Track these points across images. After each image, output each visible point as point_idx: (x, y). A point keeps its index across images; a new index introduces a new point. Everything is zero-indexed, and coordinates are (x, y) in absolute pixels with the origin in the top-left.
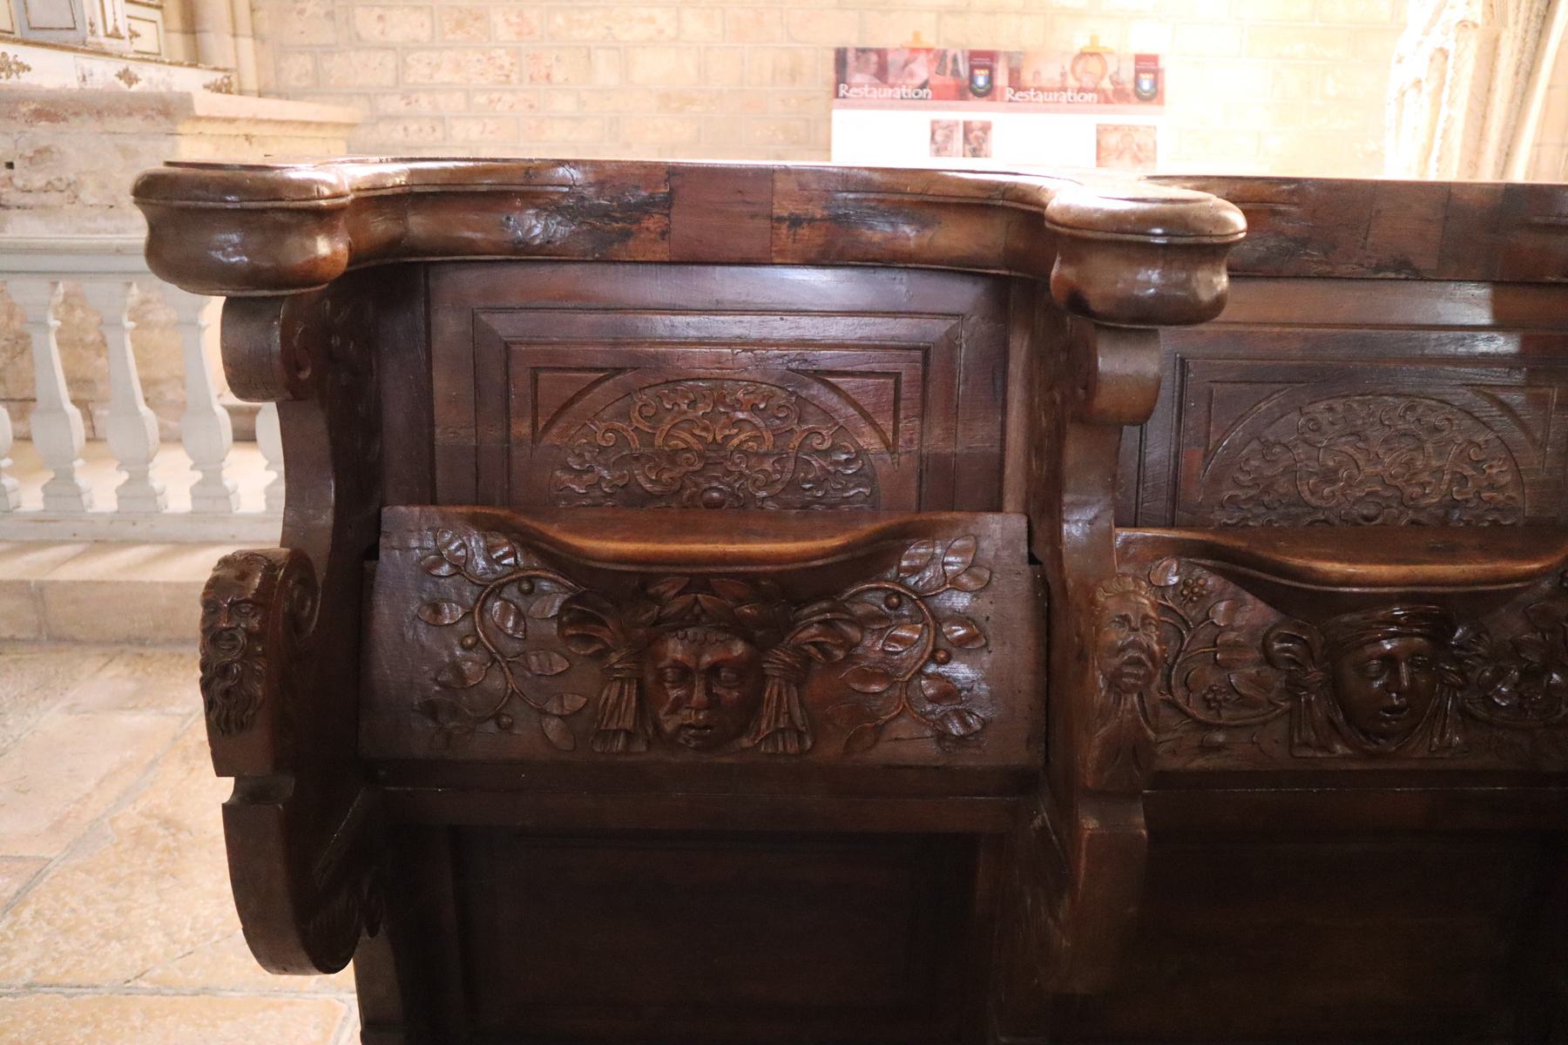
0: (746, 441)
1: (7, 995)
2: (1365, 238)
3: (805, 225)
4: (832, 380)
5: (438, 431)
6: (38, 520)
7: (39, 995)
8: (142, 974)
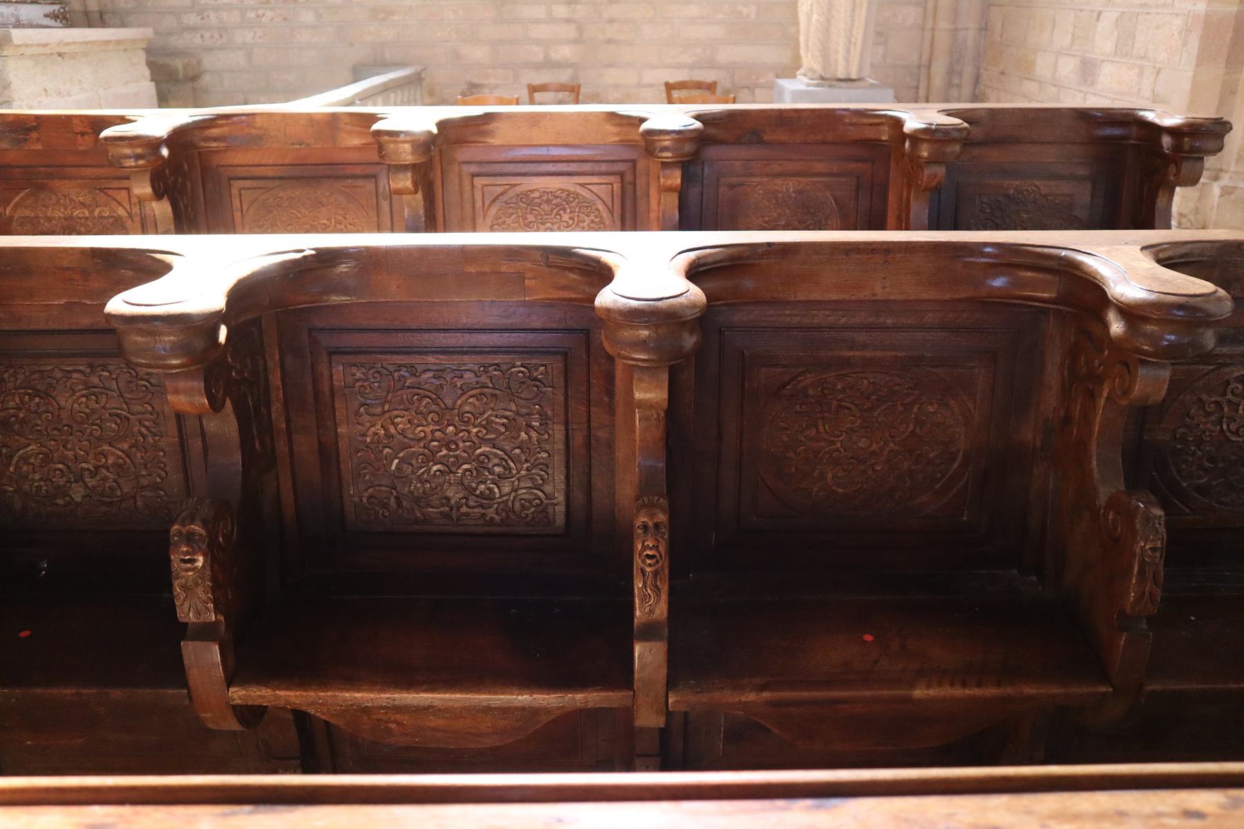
0: (79, 213)
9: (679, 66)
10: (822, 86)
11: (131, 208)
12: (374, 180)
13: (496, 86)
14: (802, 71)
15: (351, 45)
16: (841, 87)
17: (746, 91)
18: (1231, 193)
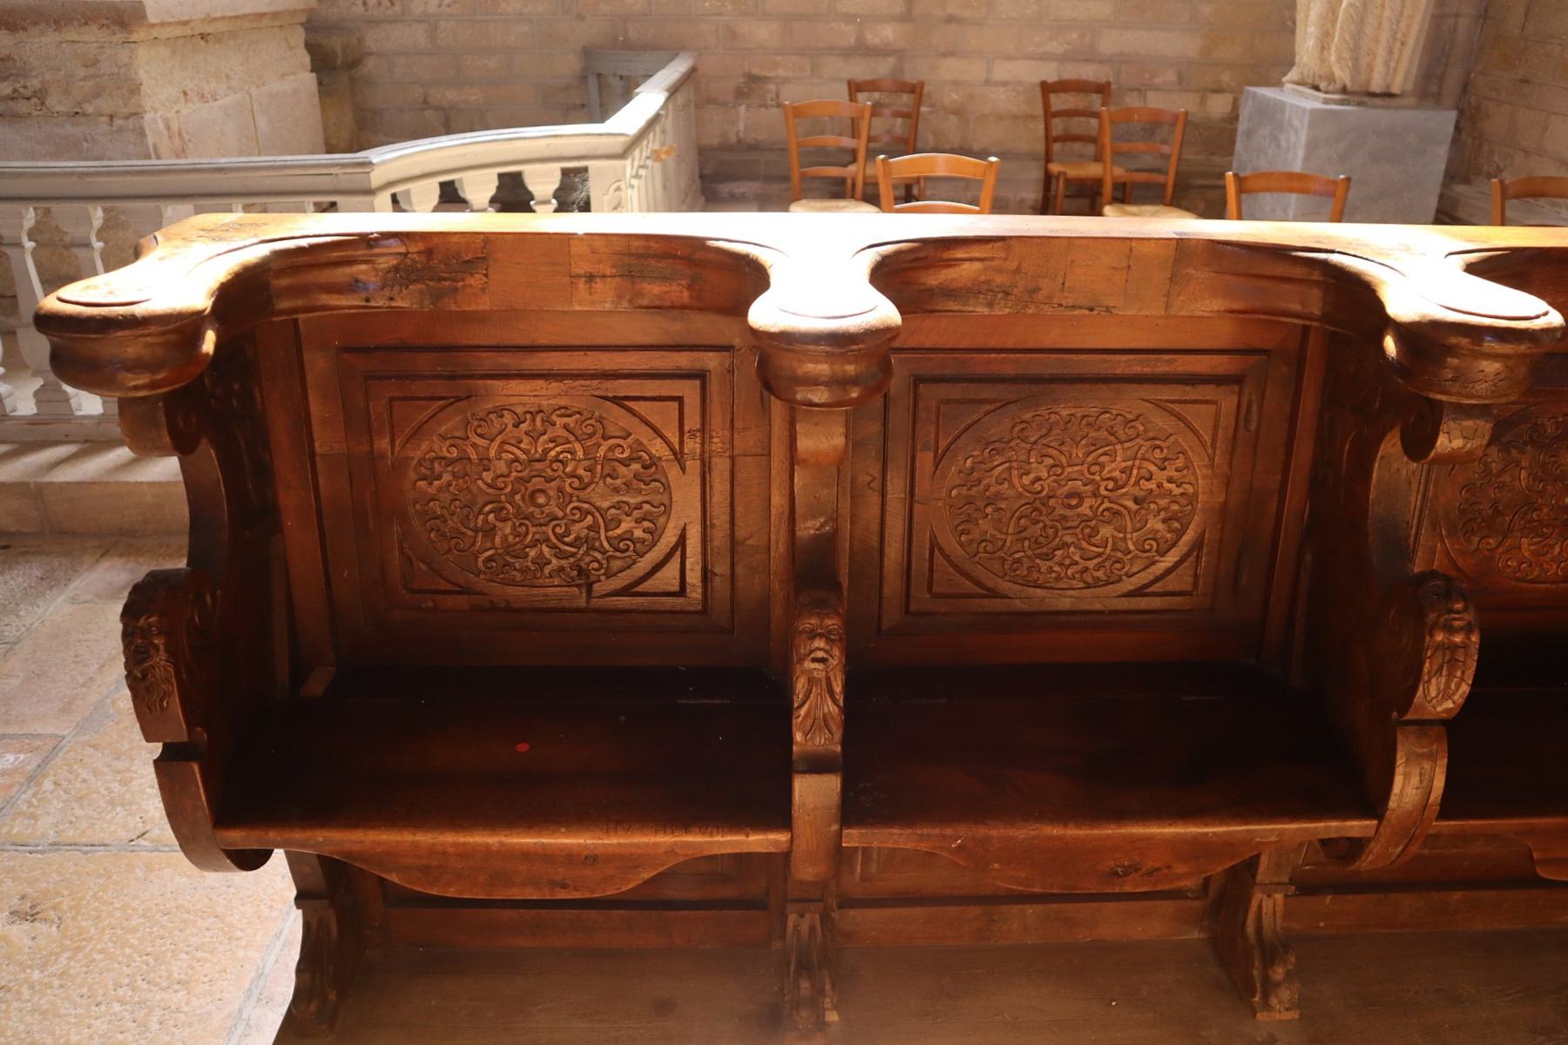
0: (562, 452)
1: (35, 852)
2: (1063, 284)
3: (598, 280)
4: (627, 403)
5: (317, 444)
6: (32, 422)
7: (60, 852)
8: (143, 834)
9: (1044, 57)
10: (1348, 104)
11: (681, 442)
12: (1236, 388)
13: (787, 80)
14: (1293, 74)
15: (580, 17)
16: (1374, 107)
17: (1135, 94)
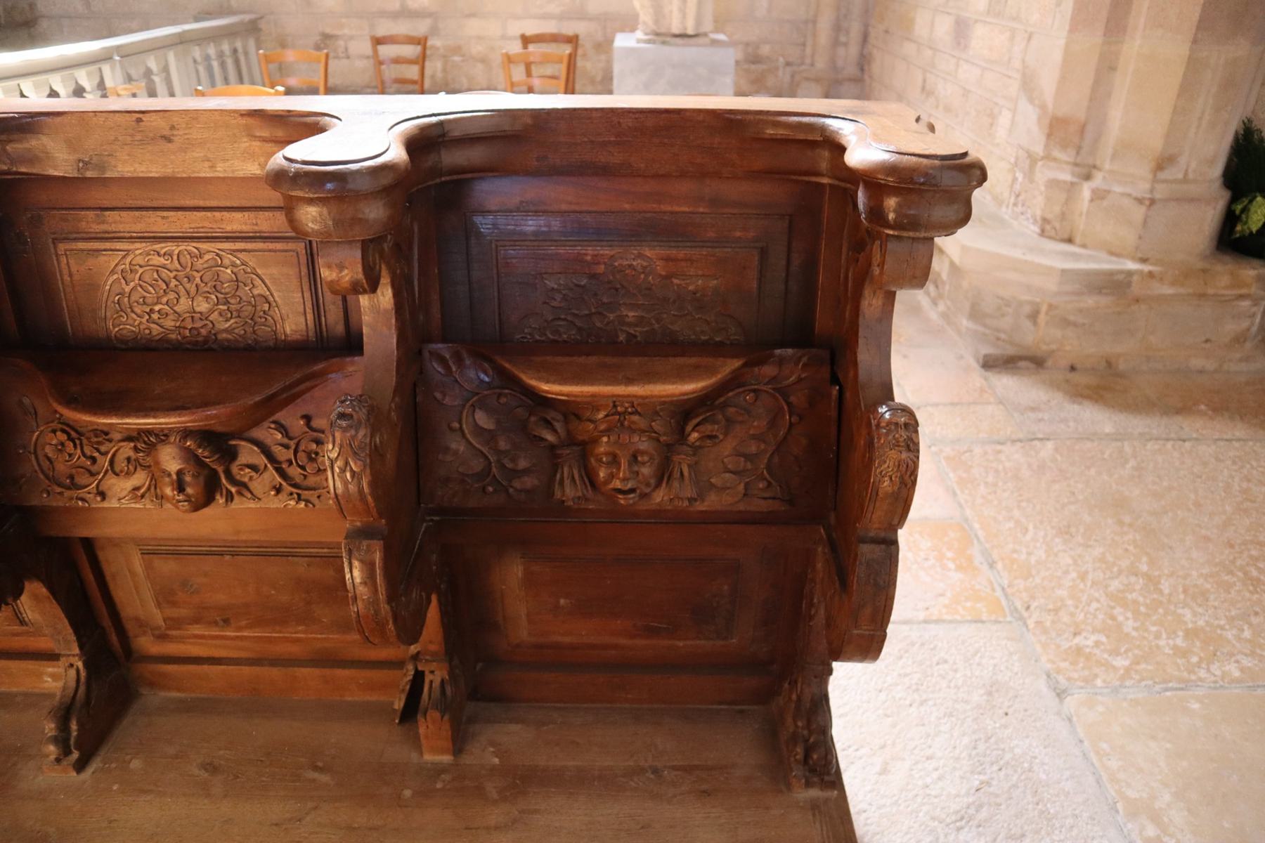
9: (545, 17)
13: (351, 38)
16: (677, 45)
18: (1102, 198)
